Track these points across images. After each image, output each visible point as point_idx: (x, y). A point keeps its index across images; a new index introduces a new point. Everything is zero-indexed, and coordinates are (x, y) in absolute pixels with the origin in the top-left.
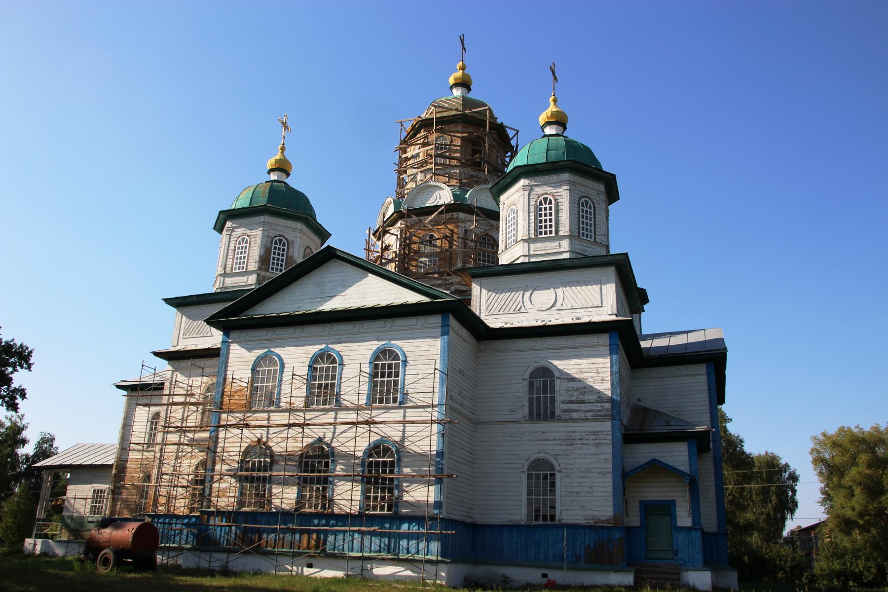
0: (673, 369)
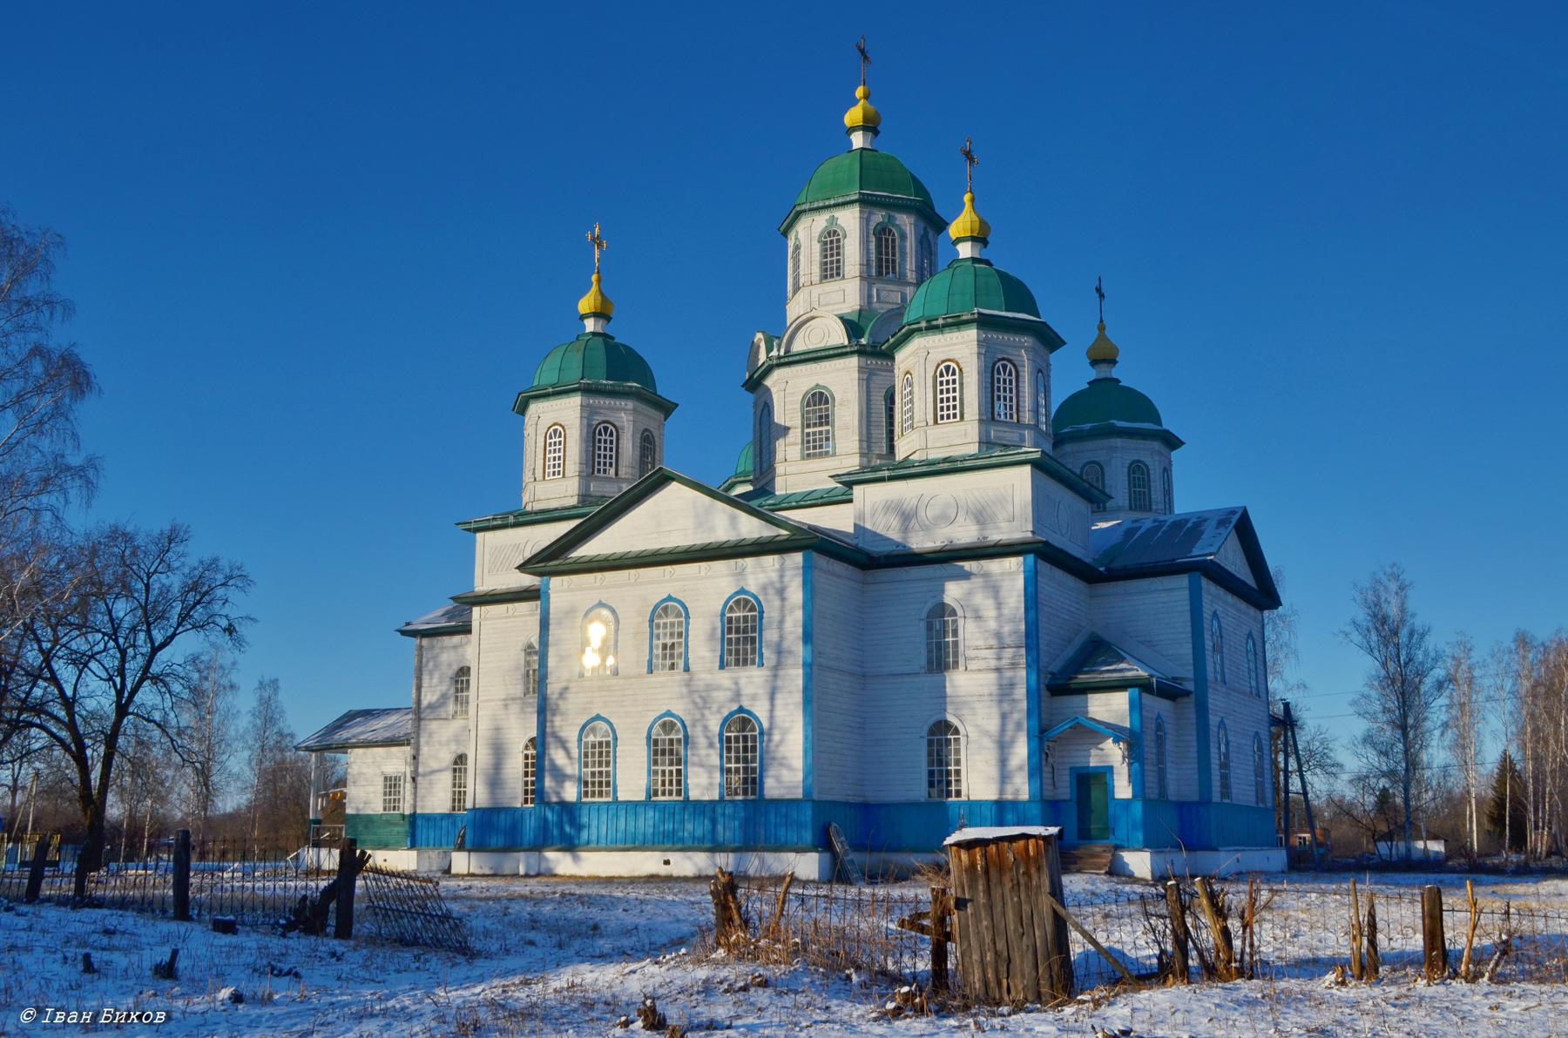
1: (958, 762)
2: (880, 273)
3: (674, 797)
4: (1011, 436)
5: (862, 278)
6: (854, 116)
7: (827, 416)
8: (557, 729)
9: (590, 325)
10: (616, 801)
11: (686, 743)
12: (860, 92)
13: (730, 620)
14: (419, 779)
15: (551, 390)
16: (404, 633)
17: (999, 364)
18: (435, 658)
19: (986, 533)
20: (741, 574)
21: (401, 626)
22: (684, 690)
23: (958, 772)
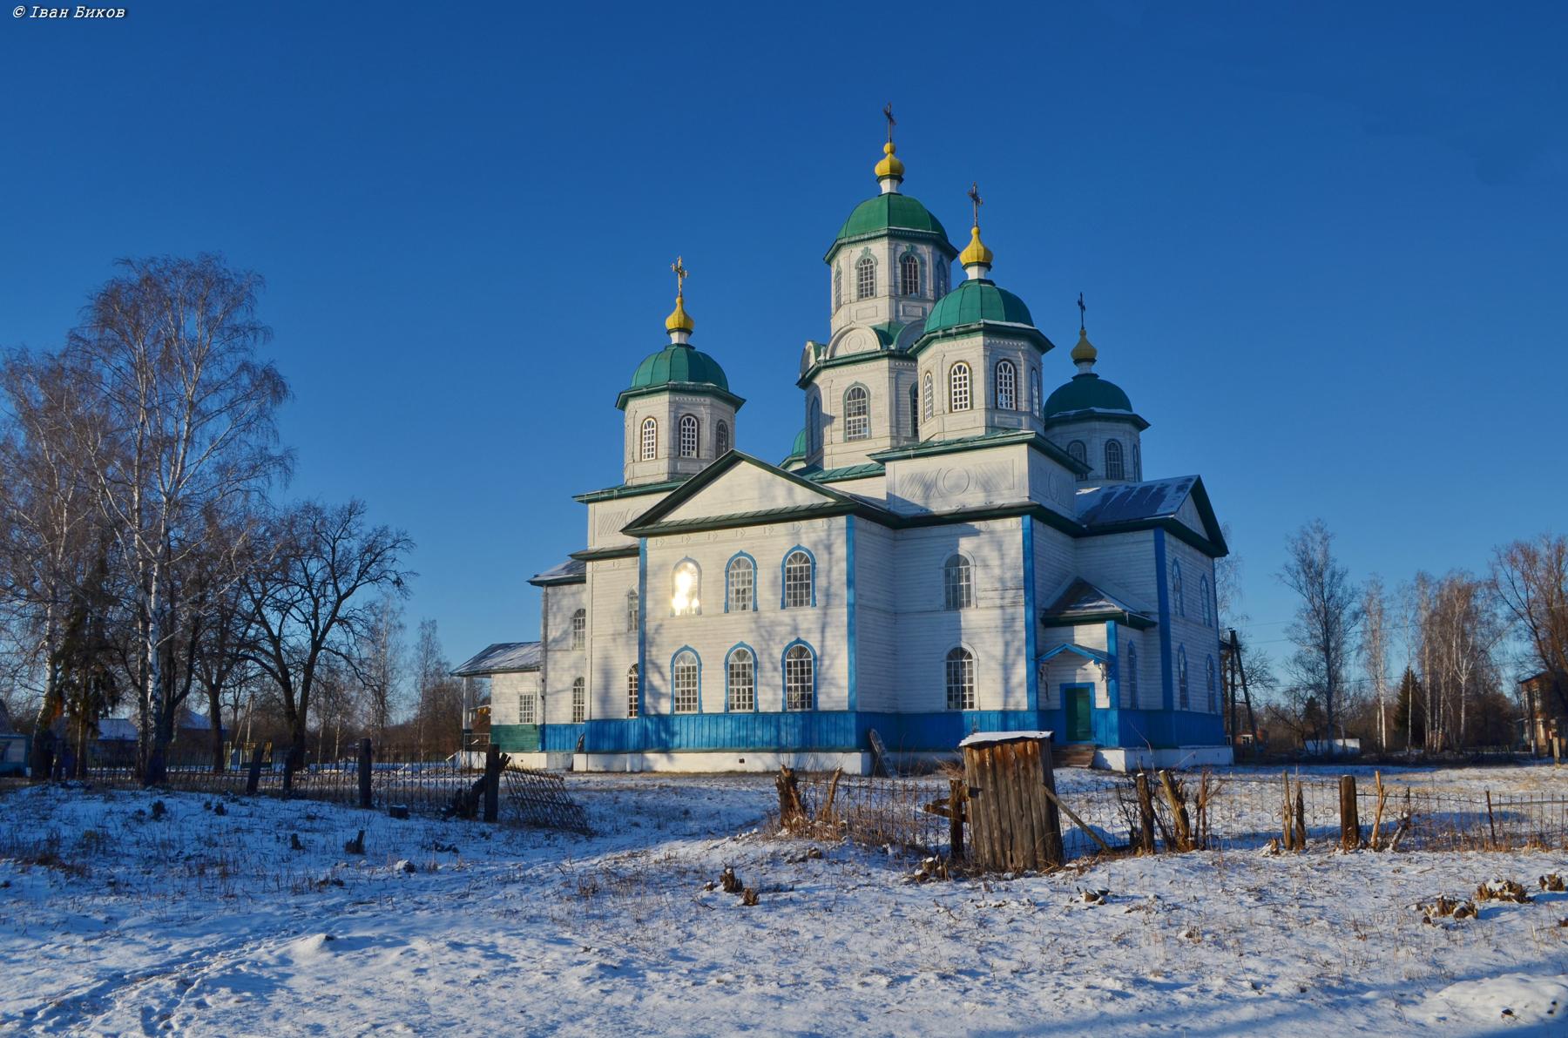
0: (1119, 537)
1: (971, 681)
2: (905, 293)
3: (747, 710)
4: (1011, 421)
5: (891, 297)
6: (883, 167)
7: (864, 407)
8: (654, 658)
9: (675, 338)
10: (701, 713)
11: (756, 667)
12: (887, 148)
13: (789, 570)
14: (547, 697)
15: (645, 390)
16: (533, 583)
17: (1001, 364)
18: (558, 602)
19: (992, 499)
20: (797, 534)
21: (531, 578)
22: (753, 626)
23: (971, 689)
